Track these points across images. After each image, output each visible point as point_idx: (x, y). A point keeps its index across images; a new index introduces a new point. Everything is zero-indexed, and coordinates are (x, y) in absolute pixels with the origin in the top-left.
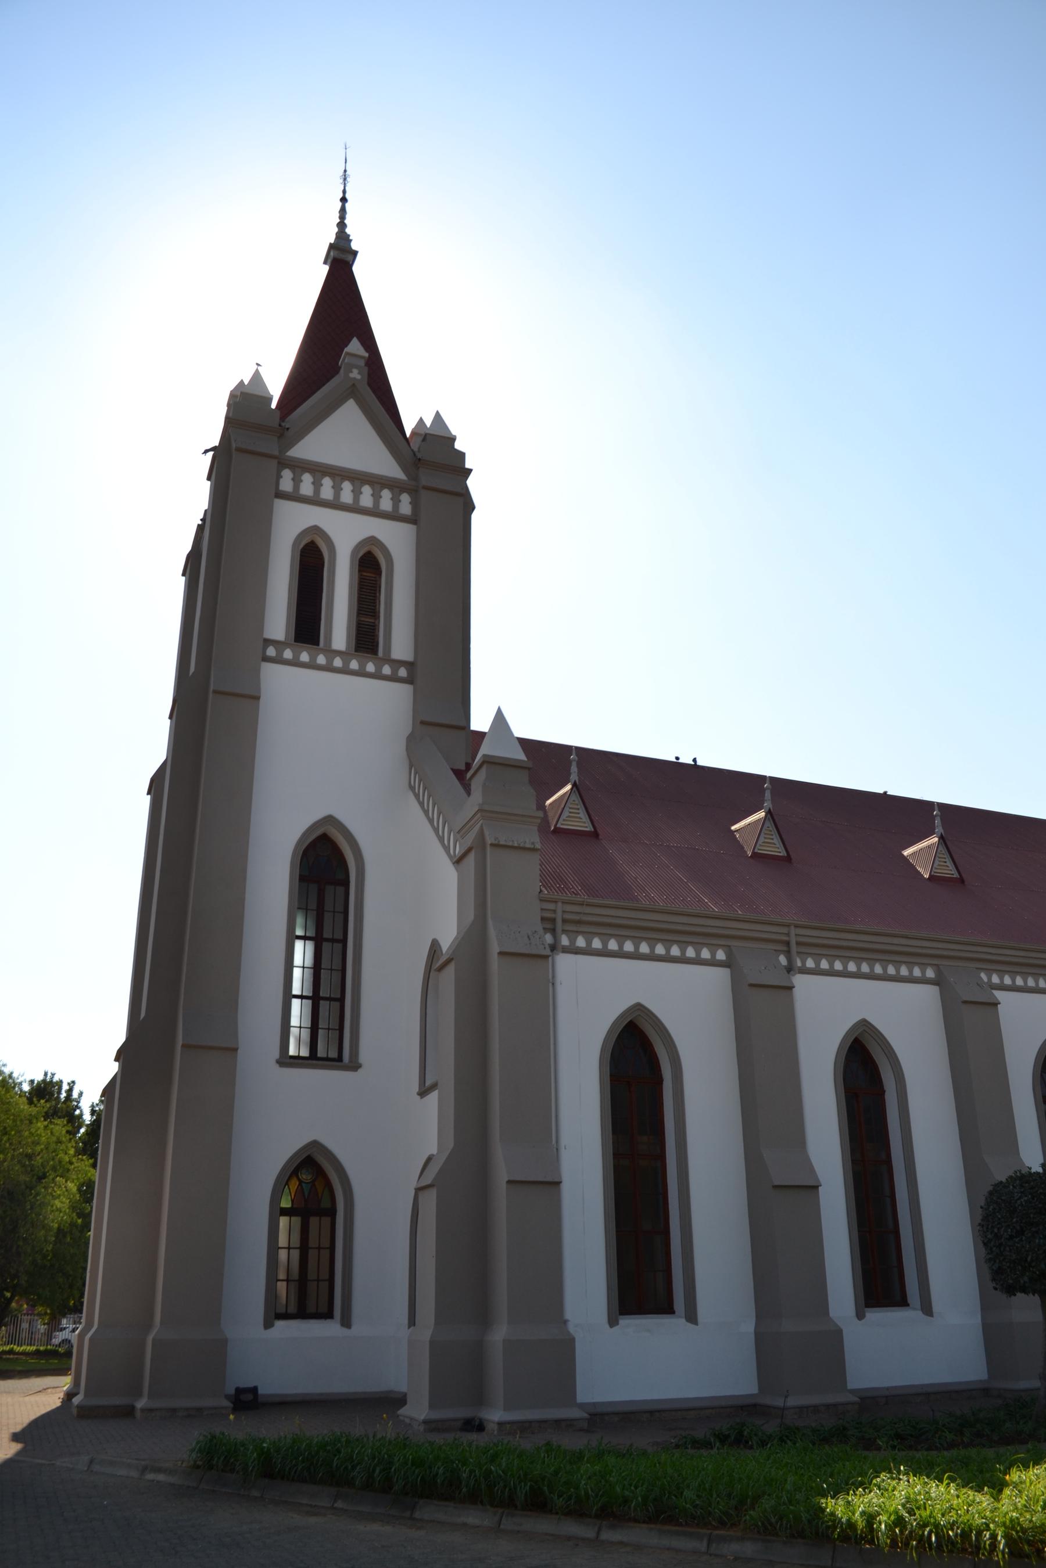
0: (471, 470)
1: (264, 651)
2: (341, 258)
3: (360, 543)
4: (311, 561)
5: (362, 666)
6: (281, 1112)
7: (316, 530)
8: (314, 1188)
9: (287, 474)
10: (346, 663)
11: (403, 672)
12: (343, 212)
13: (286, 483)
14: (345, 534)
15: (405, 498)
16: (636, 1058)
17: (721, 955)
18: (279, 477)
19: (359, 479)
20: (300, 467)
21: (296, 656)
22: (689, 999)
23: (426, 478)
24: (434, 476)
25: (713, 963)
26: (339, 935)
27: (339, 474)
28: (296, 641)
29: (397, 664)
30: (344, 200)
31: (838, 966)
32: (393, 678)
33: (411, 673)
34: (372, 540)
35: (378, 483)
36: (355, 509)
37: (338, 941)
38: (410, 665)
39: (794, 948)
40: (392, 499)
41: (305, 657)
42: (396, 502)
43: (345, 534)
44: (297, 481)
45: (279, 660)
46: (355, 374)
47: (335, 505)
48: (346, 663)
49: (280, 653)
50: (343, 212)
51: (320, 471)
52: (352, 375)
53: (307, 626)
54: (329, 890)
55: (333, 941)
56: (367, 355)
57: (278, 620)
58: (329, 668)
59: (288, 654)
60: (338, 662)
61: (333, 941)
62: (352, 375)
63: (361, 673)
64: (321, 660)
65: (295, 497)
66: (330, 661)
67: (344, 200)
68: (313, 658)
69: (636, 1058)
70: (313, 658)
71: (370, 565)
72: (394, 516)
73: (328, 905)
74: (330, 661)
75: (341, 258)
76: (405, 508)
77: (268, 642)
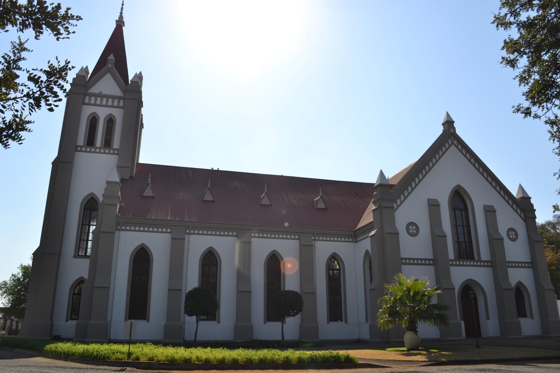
1: (76, 149)
2: (120, 24)
4: (93, 121)
7: (94, 113)
9: (87, 98)
10: (100, 151)
11: (116, 152)
12: (122, 8)
13: (87, 101)
14: (102, 113)
15: (122, 101)
16: (142, 259)
18: (84, 99)
19: (108, 97)
20: (91, 95)
21: (86, 149)
22: (158, 242)
24: (132, 94)
25: (166, 232)
30: (123, 4)
32: (114, 154)
33: (118, 152)
34: (111, 114)
35: (114, 97)
36: (107, 106)
38: (118, 150)
42: (119, 102)
43: (102, 113)
44: (90, 99)
45: (81, 151)
46: (110, 65)
48: (100, 151)
49: (81, 149)
50: (122, 8)
51: (96, 96)
53: (90, 141)
57: (81, 139)
58: (95, 152)
60: (98, 150)
65: (89, 104)
66: (95, 150)
67: (123, 4)
69: (142, 259)
71: (110, 121)
74: (95, 150)
75: (120, 24)
77: (78, 146)
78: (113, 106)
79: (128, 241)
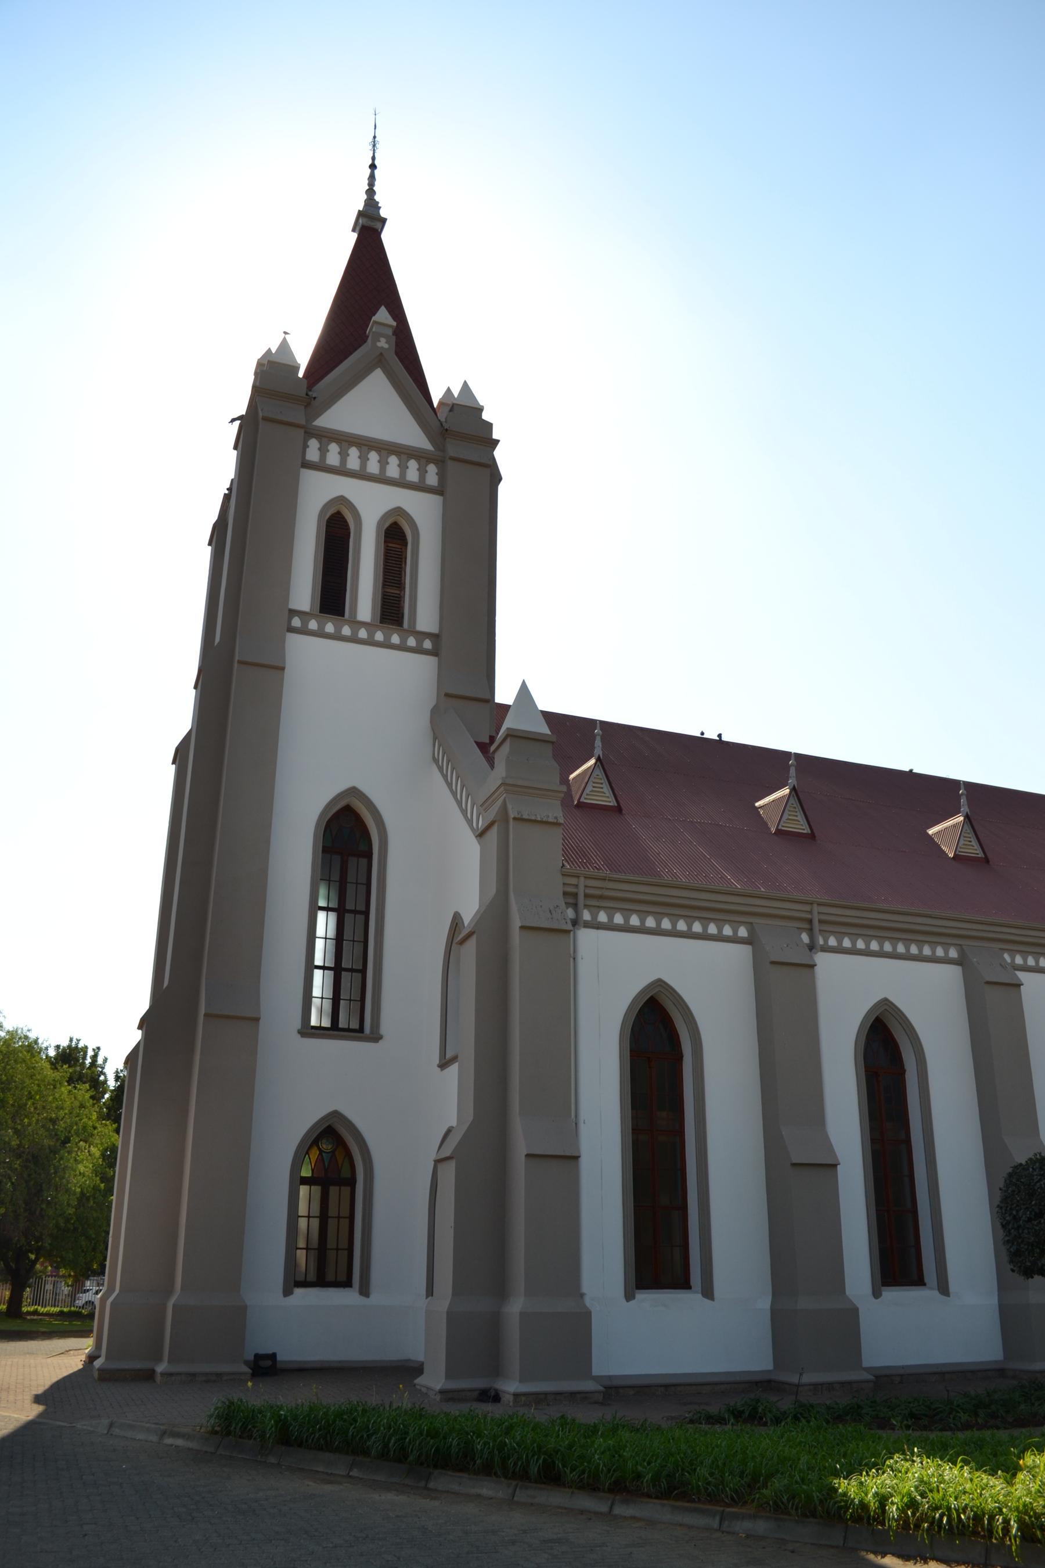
0: (498, 441)
1: (290, 621)
2: (369, 226)
3: (387, 513)
4: (337, 532)
5: (388, 638)
6: (303, 1081)
7: (342, 500)
8: (334, 1157)
9: (314, 444)
10: (371, 635)
11: (427, 644)
12: (372, 179)
13: (313, 453)
14: (371, 505)
15: (432, 469)
16: (657, 1034)
17: (743, 932)
18: (305, 446)
19: (386, 449)
20: (327, 437)
21: (321, 626)
22: (710, 976)
23: (453, 449)
24: (460, 447)
25: (734, 940)
26: (361, 907)
27: (366, 444)
28: (321, 612)
29: (422, 635)
30: (373, 167)
31: (860, 944)
32: (418, 650)
33: (436, 645)
34: (399, 511)
35: (404, 453)
36: (381, 479)
37: (360, 912)
38: (434, 637)
39: (816, 925)
40: (418, 470)
41: (330, 628)
42: (422, 472)
43: (371, 505)
44: (323, 451)
45: (304, 631)
46: (383, 343)
47: (361, 475)
48: (371, 635)
49: (305, 623)
50: (372, 179)
52: (379, 344)
53: (333, 598)
54: (352, 862)
55: (355, 912)
56: (394, 324)
57: (303, 589)
58: (354, 639)
59: (313, 625)
60: (363, 634)
61: (355, 912)
62: (379, 344)
63: (387, 645)
64: (346, 631)
65: (321, 467)
66: (355, 632)
67: (373, 167)
68: (338, 629)
69: (657, 1034)
70: (338, 629)
71: (396, 536)
72: (420, 487)
73: (351, 877)
74: (355, 632)
75: (369, 226)
76: (432, 478)
77: (293, 613)
78: (401, 483)
79: (614, 966)
